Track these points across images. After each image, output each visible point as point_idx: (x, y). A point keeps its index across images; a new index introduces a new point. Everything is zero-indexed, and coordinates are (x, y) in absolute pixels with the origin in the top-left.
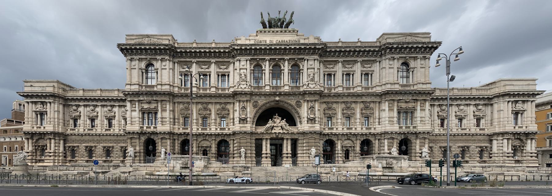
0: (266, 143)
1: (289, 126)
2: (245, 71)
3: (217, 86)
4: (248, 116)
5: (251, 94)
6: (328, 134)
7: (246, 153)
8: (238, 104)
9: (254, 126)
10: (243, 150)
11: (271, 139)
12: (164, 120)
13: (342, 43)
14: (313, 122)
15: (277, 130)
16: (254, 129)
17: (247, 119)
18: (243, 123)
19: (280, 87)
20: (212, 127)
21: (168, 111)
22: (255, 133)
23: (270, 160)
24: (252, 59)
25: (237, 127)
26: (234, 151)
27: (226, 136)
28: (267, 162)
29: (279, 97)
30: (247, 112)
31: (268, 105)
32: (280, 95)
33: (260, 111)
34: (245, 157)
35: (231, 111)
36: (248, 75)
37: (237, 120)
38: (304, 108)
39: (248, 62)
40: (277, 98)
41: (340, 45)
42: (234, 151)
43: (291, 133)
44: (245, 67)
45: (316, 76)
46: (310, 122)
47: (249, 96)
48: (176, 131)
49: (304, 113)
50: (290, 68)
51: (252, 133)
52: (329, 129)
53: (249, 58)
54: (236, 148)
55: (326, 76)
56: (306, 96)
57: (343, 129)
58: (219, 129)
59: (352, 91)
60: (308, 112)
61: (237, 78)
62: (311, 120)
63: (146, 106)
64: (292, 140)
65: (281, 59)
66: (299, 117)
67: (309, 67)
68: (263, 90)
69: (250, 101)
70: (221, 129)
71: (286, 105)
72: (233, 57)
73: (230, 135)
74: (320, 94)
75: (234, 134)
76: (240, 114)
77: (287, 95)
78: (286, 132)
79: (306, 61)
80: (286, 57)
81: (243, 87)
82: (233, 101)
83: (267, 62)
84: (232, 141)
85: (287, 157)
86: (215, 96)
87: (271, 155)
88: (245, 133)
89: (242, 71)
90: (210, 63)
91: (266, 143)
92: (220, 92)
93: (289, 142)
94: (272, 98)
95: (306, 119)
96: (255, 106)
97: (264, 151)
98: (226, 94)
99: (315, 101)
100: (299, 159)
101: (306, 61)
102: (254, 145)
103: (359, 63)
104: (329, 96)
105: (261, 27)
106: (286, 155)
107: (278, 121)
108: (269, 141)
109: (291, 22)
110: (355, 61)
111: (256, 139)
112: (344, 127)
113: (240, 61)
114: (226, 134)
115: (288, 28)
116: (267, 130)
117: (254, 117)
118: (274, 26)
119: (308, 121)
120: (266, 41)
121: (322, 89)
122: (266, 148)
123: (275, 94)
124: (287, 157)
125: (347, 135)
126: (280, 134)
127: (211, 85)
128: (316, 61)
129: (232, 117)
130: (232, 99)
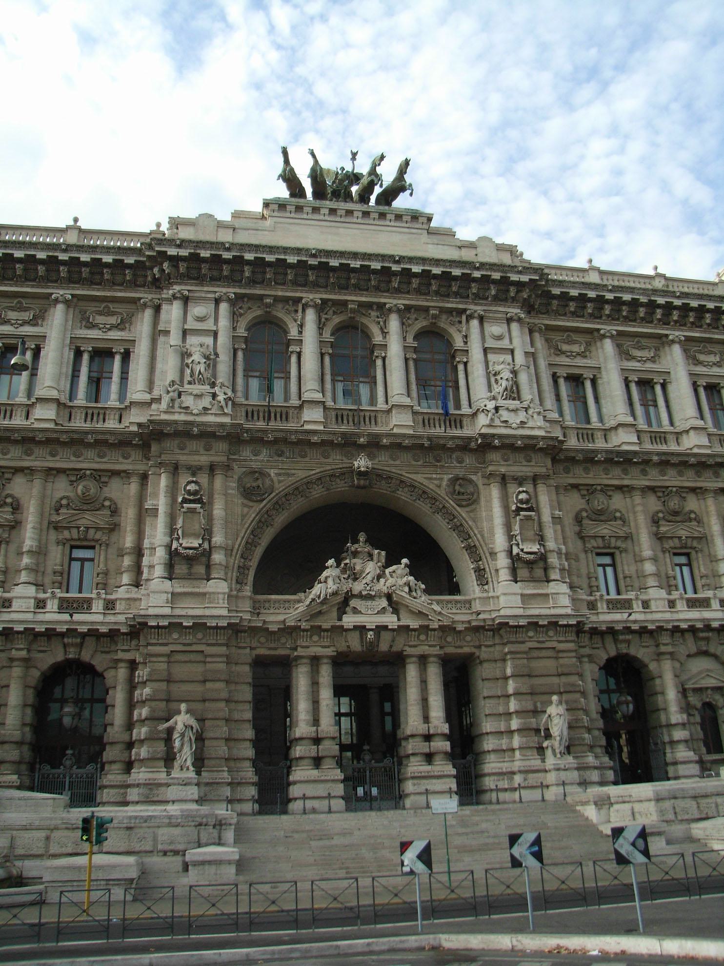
0: (315, 684)
1: (427, 591)
2: (209, 341)
3: (64, 399)
4: (218, 539)
5: (235, 438)
6: (611, 631)
7: (200, 738)
8: (164, 481)
9: (248, 591)
10: (182, 720)
11: (340, 661)
13: (602, 273)
14: (539, 572)
15: (370, 615)
16: (247, 606)
17: (208, 554)
18: (190, 577)
19: (374, 417)
20: (18, 591)
22: (254, 630)
23: (338, 774)
24: (239, 297)
25: (156, 598)
26: (130, 726)
27: (90, 642)
28: (321, 790)
29: (371, 457)
30: (210, 519)
31: (317, 492)
32: (374, 445)
33: (281, 520)
34: (199, 762)
35: (129, 515)
36: (224, 358)
37: (156, 560)
38: (490, 509)
39: (224, 307)
40: (362, 463)
41: (594, 278)
42: (130, 726)
43: (442, 628)
44: (209, 325)
45: (523, 378)
46: (523, 573)
47: (223, 446)
49: (492, 533)
50: (410, 339)
51: (235, 629)
52: (614, 605)
53: (232, 291)
54: (145, 712)
55: (561, 381)
56: (494, 456)
57: (672, 604)
58: (52, 605)
59: (673, 447)
60: (508, 527)
61: (168, 367)
62: (530, 568)
64: (446, 662)
65: (369, 306)
66: (472, 550)
67: (491, 343)
68: (292, 425)
69: (228, 468)
70: (66, 605)
71: (403, 495)
72: (157, 284)
73: (113, 634)
74: (554, 452)
75: (138, 629)
76: (172, 530)
77: (407, 448)
78: (414, 624)
79: (475, 323)
80: (390, 301)
81: (196, 406)
82: (141, 467)
83: (311, 316)
84: (122, 672)
85: (429, 757)
86: (48, 442)
87: (343, 748)
88: (199, 626)
89: (192, 340)
90: (48, 301)
91: (315, 684)
92: (79, 423)
93: (434, 674)
94: (336, 461)
95: (503, 561)
96: (250, 494)
97: (302, 728)
98: (111, 432)
99: (535, 479)
100: (491, 764)
101: (475, 323)
102: (246, 693)
103: (677, 349)
104: (589, 459)
105: (282, 191)
106: (424, 747)
107: (371, 568)
108: (326, 675)
109: (403, 189)
110: (659, 337)
111: (259, 663)
112: (675, 595)
113: (186, 300)
114: (93, 633)
115: (389, 203)
116: (315, 613)
117: (250, 545)
118: (336, 194)
119: (514, 571)
121: (558, 433)
122: (316, 711)
123: (349, 445)
124: (429, 757)
125: (692, 630)
126: (386, 637)
127: (39, 392)
128: (515, 326)
129: (129, 541)
130: (136, 455)
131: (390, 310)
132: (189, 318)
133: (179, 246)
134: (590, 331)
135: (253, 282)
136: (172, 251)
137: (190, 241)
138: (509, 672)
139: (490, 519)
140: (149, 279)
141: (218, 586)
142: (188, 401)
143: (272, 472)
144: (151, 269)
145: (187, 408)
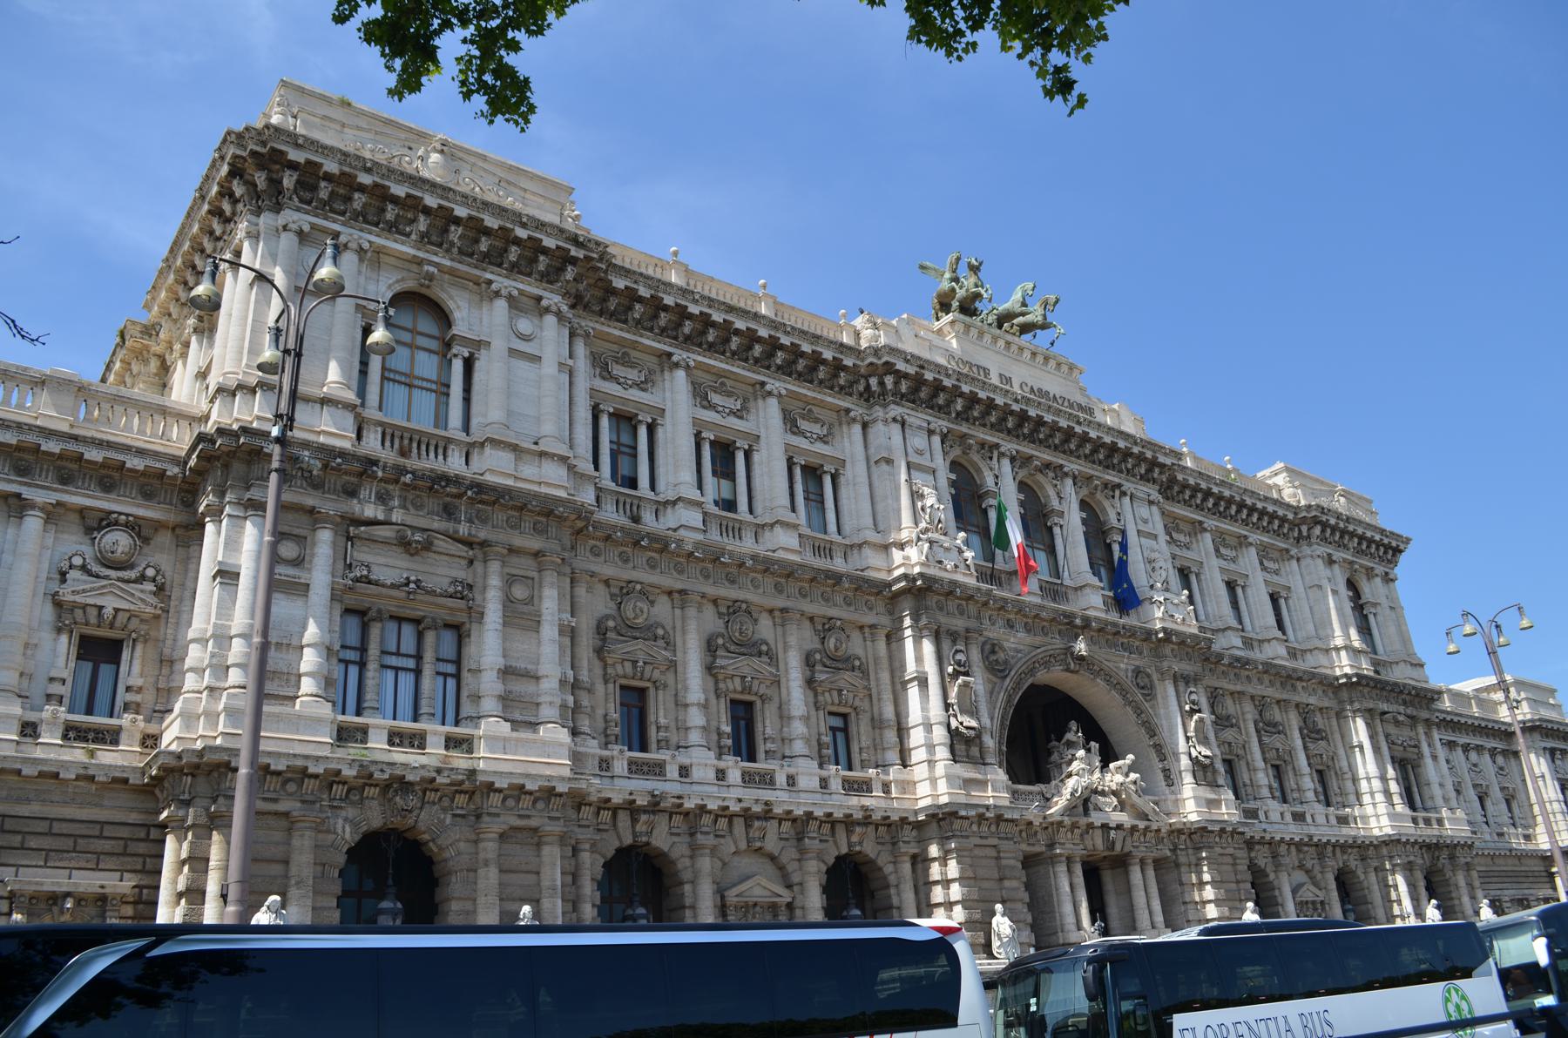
8: (928, 647)
12: (521, 687)
21: (549, 631)
38: (1167, 707)
39: (936, 440)
40: (1081, 647)
48: (596, 786)
49: (1173, 734)
53: (942, 424)
56: (1167, 650)
63: (388, 567)
65: (1048, 465)
72: (867, 396)
76: (947, 706)
79: (1127, 500)
84: (906, 867)
95: (1185, 762)
101: (1127, 500)
120: (986, 372)
129: (889, 712)
131: (1066, 474)
132: (910, 450)
133: (907, 361)
134: (1193, 522)
135: (962, 416)
136: (901, 366)
137: (919, 358)
138: (1207, 877)
139: (1169, 718)
140: (861, 388)
141: (1000, 775)
142: (941, 555)
143: (1006, 645)
144: (866, 378)
145: (940, 562)
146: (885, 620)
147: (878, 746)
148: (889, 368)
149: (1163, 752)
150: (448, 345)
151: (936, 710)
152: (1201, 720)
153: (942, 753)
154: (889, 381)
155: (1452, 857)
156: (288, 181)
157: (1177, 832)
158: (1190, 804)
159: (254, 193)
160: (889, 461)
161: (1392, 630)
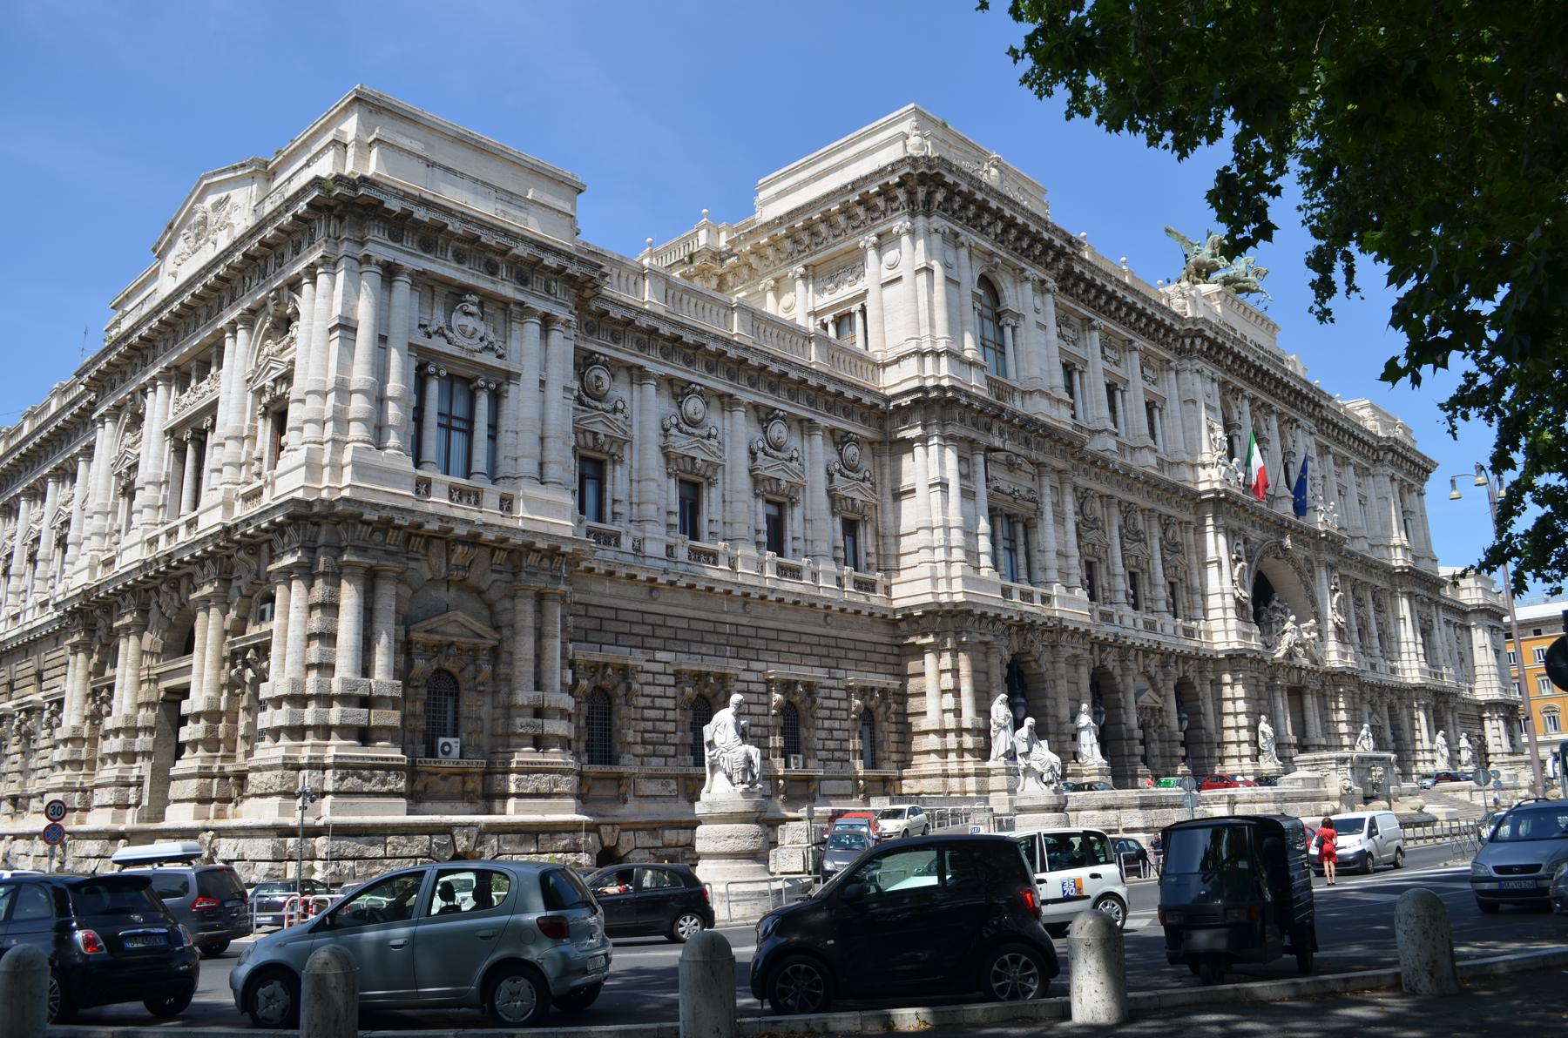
146: (1192, 518)
147: (1192, 607)
148: (1200, 333)
149: (1319, 617)
150: (998, 316)
151: (1227, 586)
152: (1242, 568)
153: (1231, 614)
154: (1198, 342)
155: (1446, 702)
156: (939, 196)
157: (1326, 673)
158: (1334, 656)
159: (911, 200)
160: (1194, 402)
161: (1421, 533)
